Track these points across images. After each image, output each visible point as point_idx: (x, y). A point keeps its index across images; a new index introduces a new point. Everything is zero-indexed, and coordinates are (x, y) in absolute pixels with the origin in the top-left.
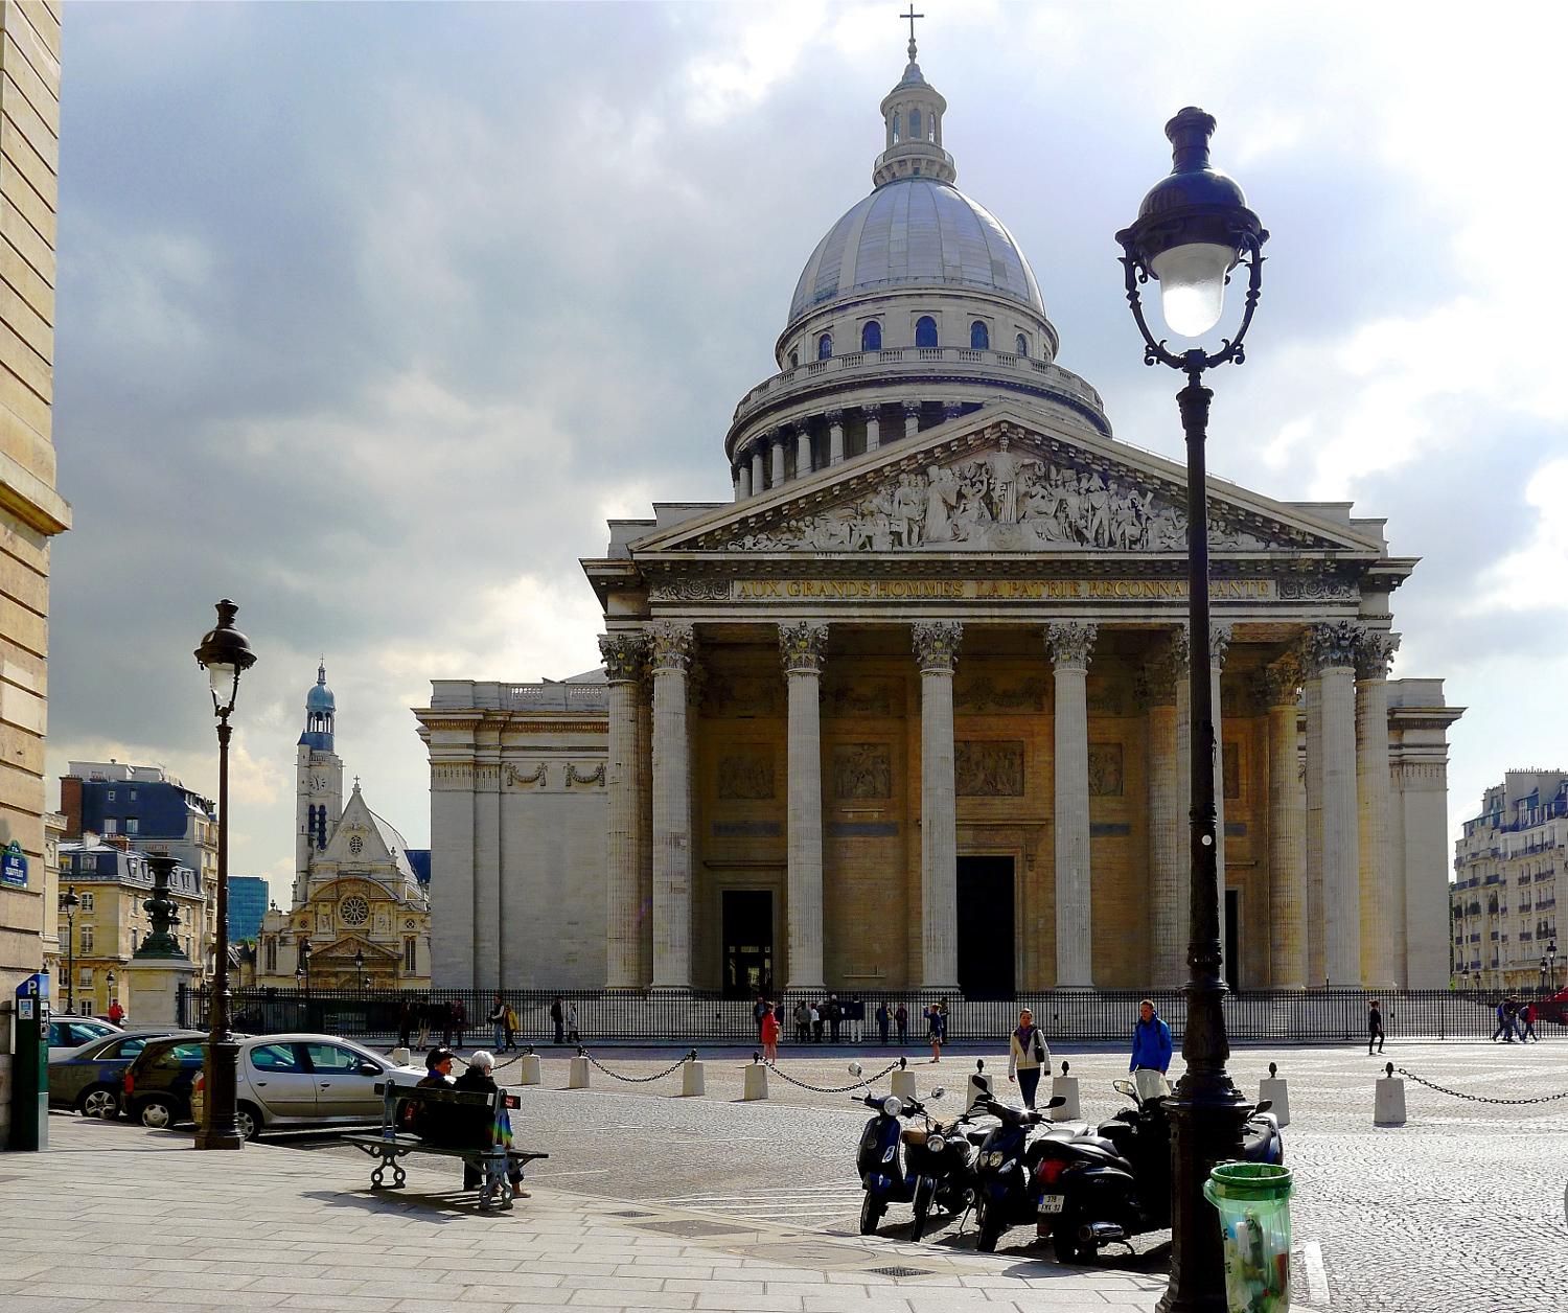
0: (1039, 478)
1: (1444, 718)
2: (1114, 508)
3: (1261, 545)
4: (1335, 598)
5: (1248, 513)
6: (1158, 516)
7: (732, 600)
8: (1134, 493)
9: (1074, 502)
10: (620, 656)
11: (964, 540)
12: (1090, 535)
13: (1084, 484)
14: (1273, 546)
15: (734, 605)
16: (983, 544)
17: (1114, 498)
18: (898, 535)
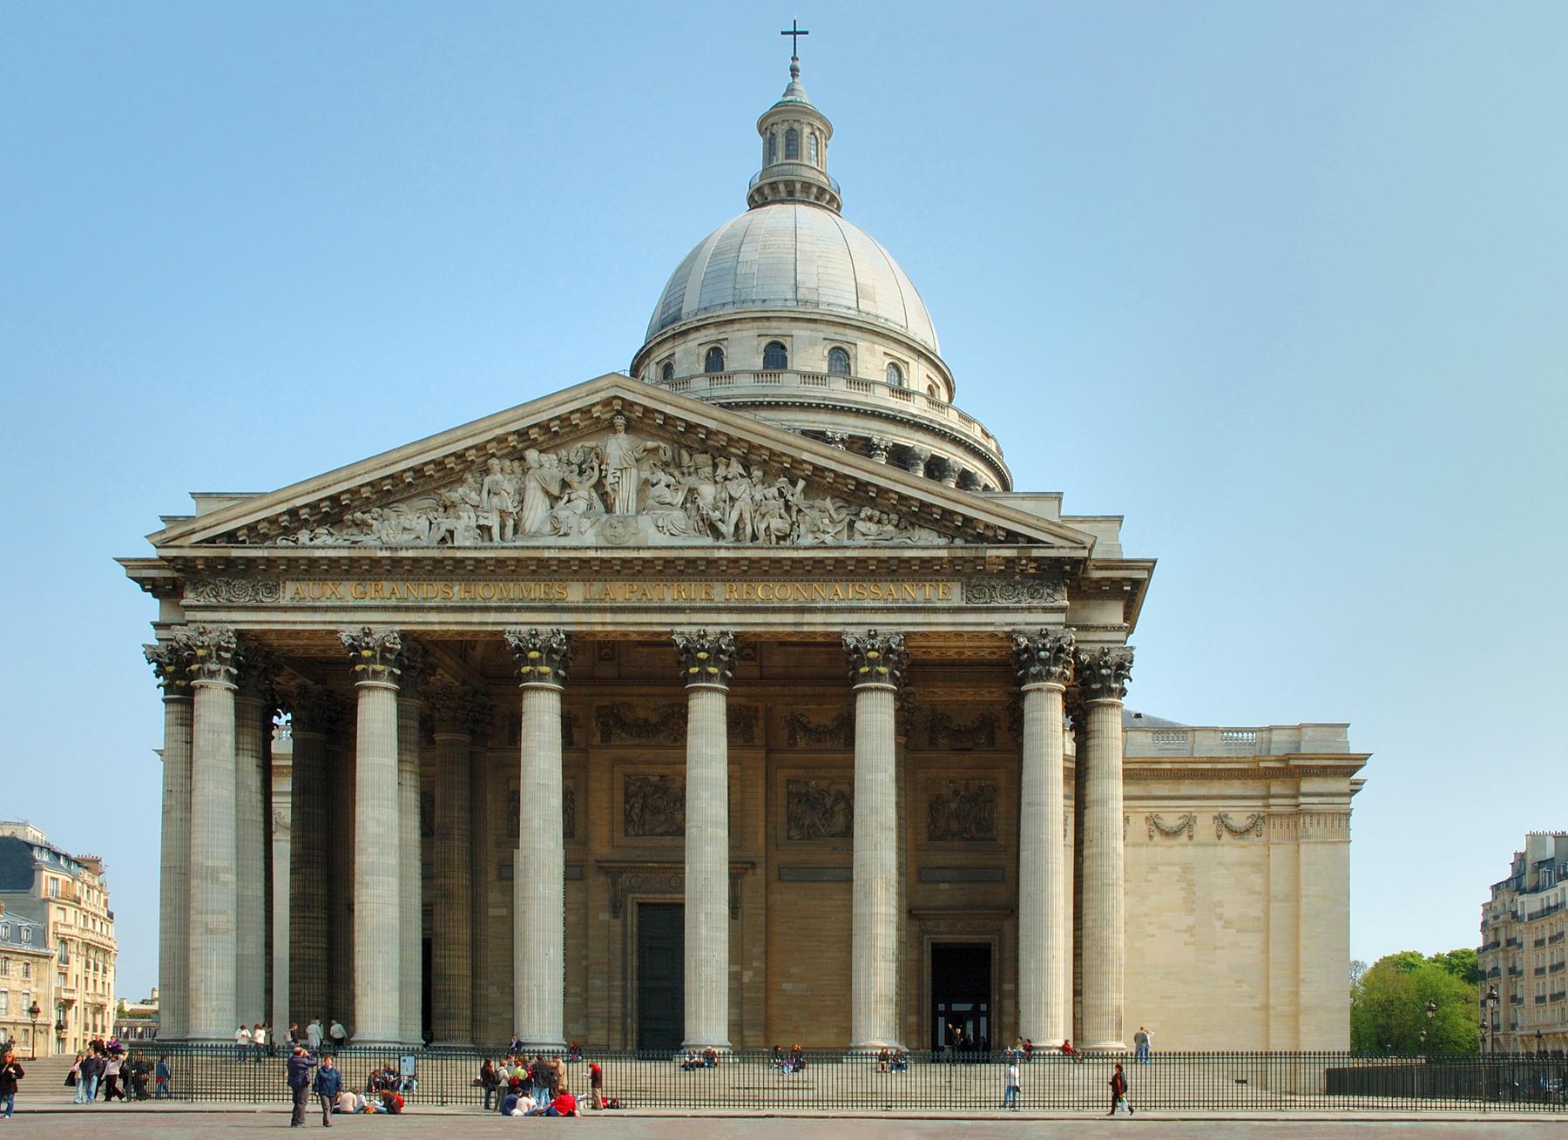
0: (666, 464)
1: (1346, 767)
2: (758, 497)
3: (943, 541)
4: (1035, 603)
5: (922, 504)
6: (812, 507)
7: (285, 601)
8: (782, 481)
9: (708, 492)
10: (170, 669)
11: (565, 535)
12: (727, 529)
13: (721, 471)
14: (958, 542)
15: (285, 609)
16: (590, 538)
17: (759, 487)
18: (489, 529)
